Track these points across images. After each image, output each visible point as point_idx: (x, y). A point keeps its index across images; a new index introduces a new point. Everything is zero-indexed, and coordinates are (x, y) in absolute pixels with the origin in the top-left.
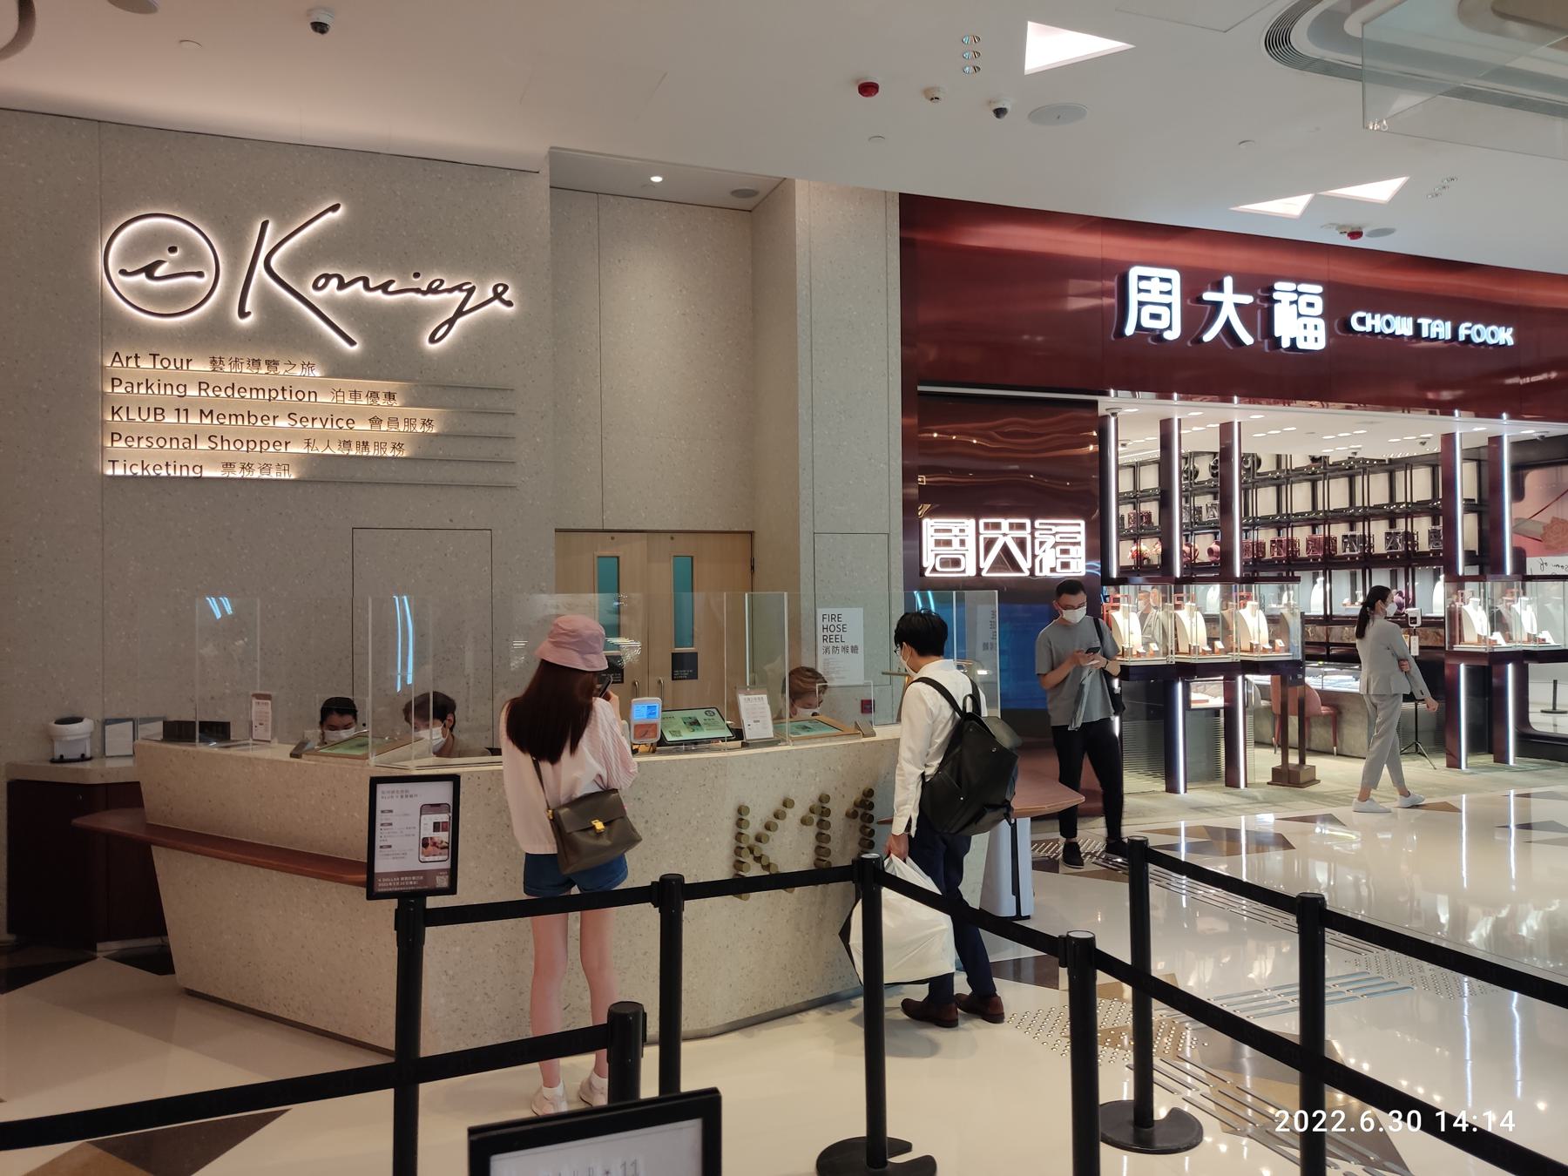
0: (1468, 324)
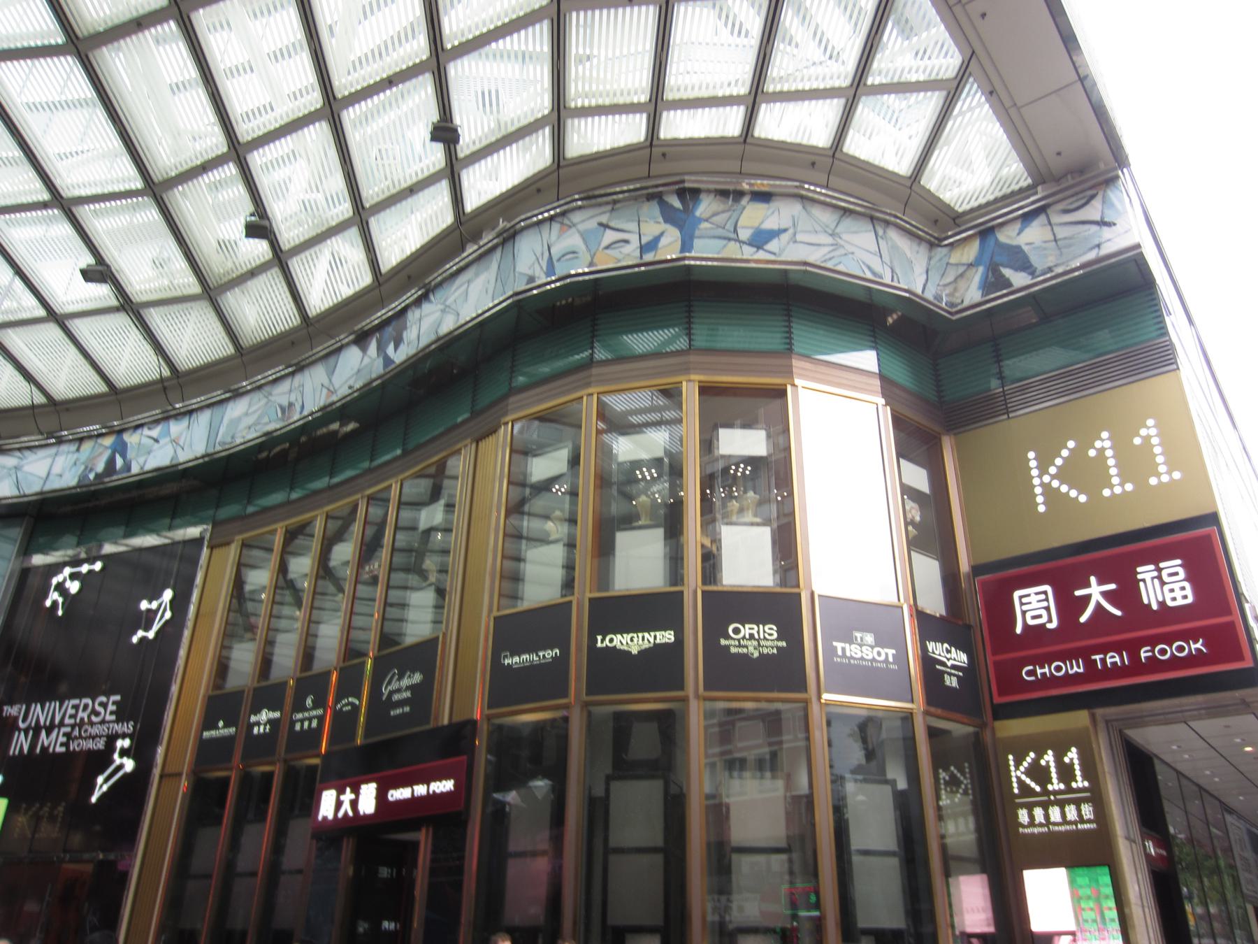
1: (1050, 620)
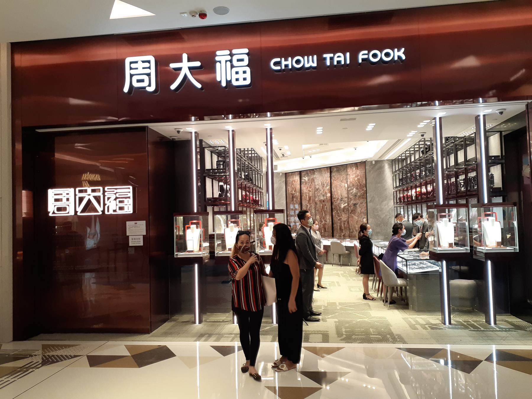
0: (366, 52)
1: (150, 85)
